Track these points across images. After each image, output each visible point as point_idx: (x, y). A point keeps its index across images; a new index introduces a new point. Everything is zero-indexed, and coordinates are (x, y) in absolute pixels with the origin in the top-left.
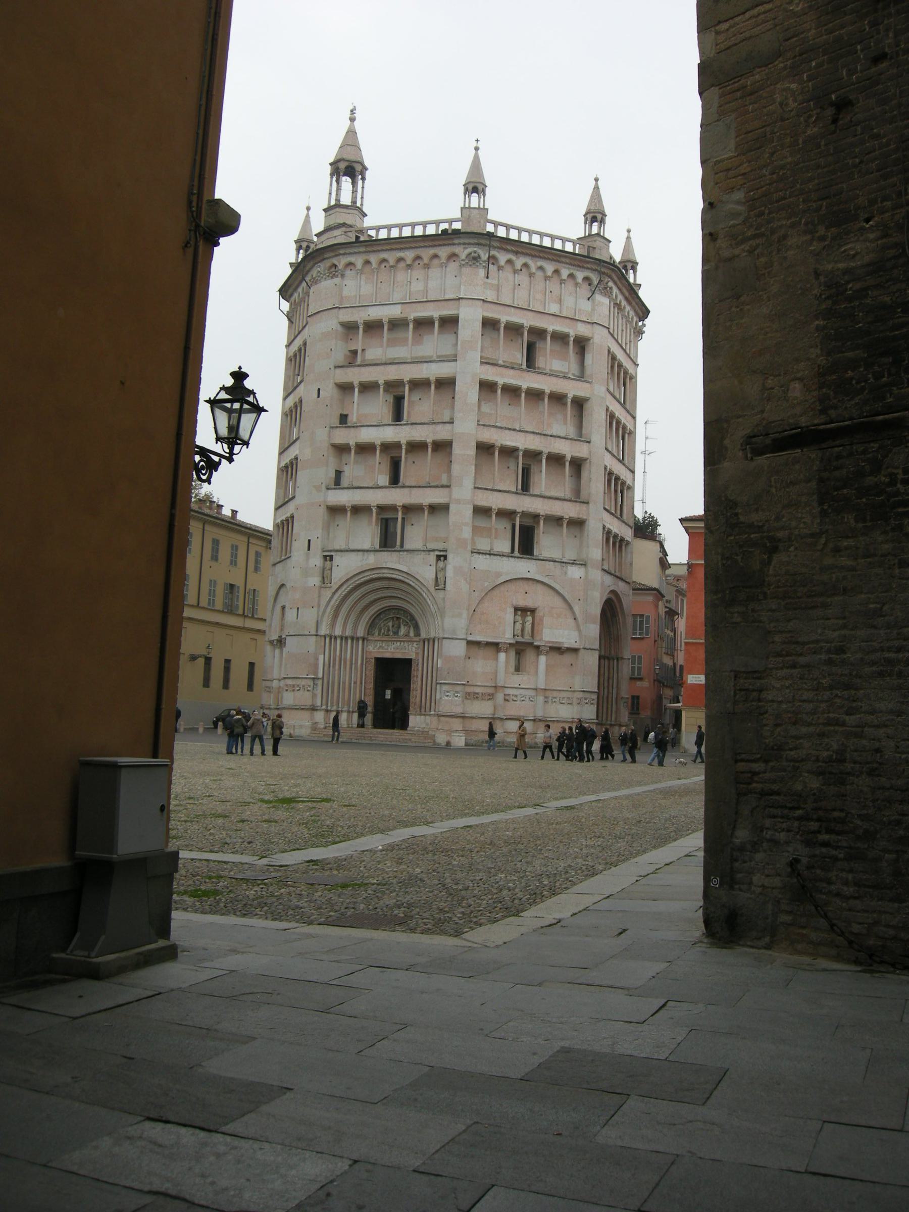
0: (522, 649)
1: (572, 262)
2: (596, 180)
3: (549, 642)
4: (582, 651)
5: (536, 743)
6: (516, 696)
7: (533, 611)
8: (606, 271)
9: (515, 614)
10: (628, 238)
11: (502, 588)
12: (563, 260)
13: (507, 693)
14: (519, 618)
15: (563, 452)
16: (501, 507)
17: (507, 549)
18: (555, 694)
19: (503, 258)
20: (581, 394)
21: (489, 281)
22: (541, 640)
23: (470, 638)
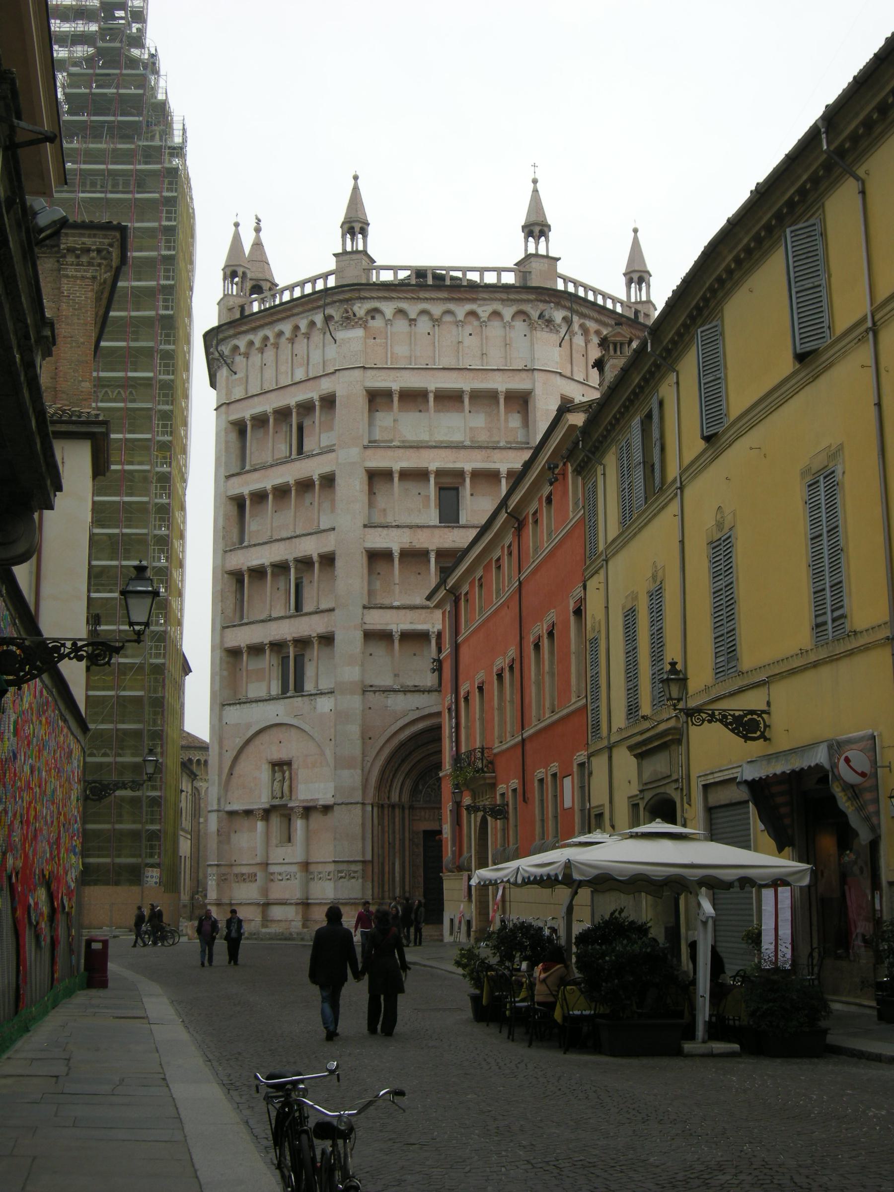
0: (279, 812)
1: (306, 308)
2: (356, 178)
3: (303, 801)
4: (336, 808)
5: (291, 934)
6: (280, 874)
7: (289, 764)
8: (347, 296)
9: (274, 772)
10: (535, 191)
11: (257, 742)
12: (295, 311)
13: (272, 871)
14: (278, 776)
15: (308, 553)
16: (248, 642)
17: (275, 689)
18: (320, 868)
19: (241, 343)
20: (326, 469)
21: (237, 376)
22: (297, 799)
23: (229, 808)
